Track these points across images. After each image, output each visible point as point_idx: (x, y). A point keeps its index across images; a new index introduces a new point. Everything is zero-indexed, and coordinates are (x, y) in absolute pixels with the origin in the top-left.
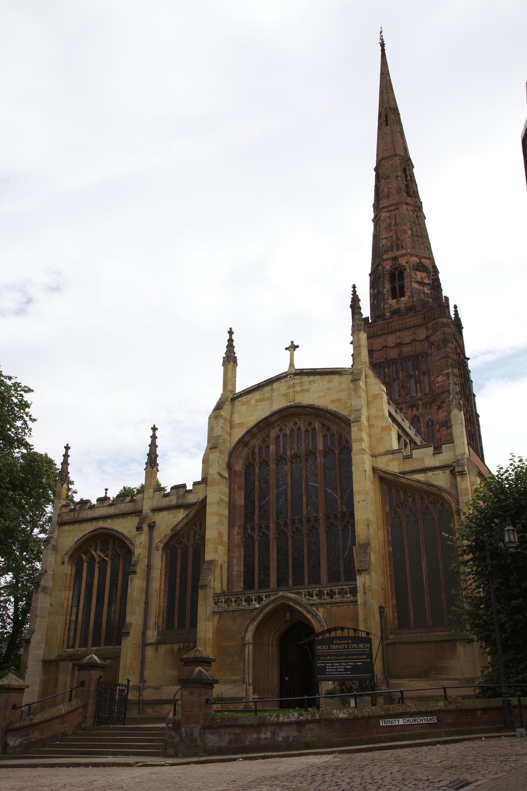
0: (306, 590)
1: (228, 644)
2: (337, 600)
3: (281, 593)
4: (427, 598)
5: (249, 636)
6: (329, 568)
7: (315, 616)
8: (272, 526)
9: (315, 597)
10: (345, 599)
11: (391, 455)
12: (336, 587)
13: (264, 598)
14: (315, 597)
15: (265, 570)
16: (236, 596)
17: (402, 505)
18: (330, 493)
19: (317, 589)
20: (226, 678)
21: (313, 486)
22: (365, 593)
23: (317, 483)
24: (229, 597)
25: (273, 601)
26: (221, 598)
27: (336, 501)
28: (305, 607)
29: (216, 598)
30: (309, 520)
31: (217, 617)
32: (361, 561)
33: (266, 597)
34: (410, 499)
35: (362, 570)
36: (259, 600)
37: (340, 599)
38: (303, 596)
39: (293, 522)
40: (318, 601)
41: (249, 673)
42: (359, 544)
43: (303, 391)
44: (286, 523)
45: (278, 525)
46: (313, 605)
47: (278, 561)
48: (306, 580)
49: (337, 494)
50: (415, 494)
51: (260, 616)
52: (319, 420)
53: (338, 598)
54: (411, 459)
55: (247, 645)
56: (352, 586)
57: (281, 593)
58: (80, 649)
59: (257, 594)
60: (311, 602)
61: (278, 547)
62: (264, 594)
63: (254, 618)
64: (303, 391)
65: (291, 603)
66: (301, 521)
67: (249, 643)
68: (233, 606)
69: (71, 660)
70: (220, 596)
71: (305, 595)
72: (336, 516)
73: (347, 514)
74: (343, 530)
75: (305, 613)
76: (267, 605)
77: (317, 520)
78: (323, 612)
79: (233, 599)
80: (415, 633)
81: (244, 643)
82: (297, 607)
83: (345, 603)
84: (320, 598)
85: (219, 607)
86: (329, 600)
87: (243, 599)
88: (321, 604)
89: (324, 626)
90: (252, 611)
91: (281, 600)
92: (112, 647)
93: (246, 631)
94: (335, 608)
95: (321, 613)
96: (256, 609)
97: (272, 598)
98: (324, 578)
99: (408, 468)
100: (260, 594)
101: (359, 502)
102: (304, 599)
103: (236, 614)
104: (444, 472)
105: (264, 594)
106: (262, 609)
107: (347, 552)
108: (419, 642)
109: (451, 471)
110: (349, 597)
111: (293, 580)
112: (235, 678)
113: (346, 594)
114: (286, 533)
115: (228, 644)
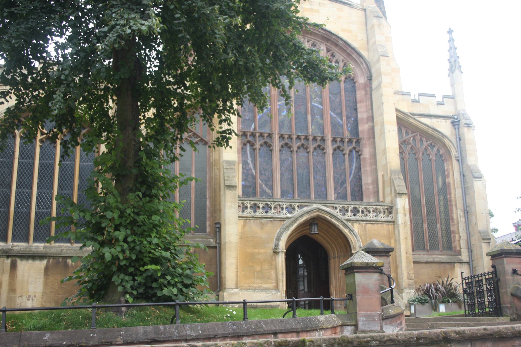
0: (341, 206)
1: (256, 251)
2: (372, 218)
3: (315, 206)
4: (425, 226)
5: (282, 245)
6: (335, 189)
7: (351, 230)
8: (276, 137)
9: (349, 213)
10: (379, 218)
11: (400, 96)
12: (371, 207)
13: (296, 209)
14: (349, 213)
15: (269, 181)
16: (264, 203)
17: (405, 142)
18: (335, 118)
19: (352, 206)
20: (255, 285)
21: (316, 106)
22: (405, 214)
23: (321, 104)
24: (256, 202)
25: (308, 212)
26: (245, 202)
27: (342, 126)
28: (342, 221)
29: (240, 202)
30: (315, 139)
31: (242, 222)
32: (399, 186)
33: (298, 206)
34: (412, 138)
35: (402, 194)
36: (291, 209)
37: (375, 218)
38: (338, 210)
39: (298, 138)
40: (353, 218)
41: (282, 281)
42: (391, 170)
43: (312, 10)
44: (290, 137)
45: (282, 137)
46: (348, 220)
47: (281, 174)
48: (313, 196)
49: (342, 120)
50: (416, 135)
51: (293, 225)
52: (326, 44)
53: (371, 216)
54: (418, 103)
55: (280, 254)
56: (386, 207)
57: (315, 206)
58: (15, 244)
59: (289, 204)
60: (346, 217)
61: (280, 160)
62: (297, 204)
63: (288, 227)
64: (312, 10)
65: (326, 217)
66: (306, 138)
67: (282, 252)
68: (260, 213)
69: (8, 257)
70: (245, 200)
71: (340, 210)
72: (342, 141)
73: (354, 140)
74: (349, 155)
75: (341, 227)
76: (302, 216)
77: (323, 140)
78: (359, 228)
79: (261, 206)
80: (419, 255)
81: (278, 251)
82: (334, 221)
83: (379, 221)
84: (355, 215)
85: (243, 211)
86: (364, 218)
87: (273, 207)
88: (357, 221)
89: (359, 241)
90: (283, 219)
91: (316, 212)
92: (69, 245)
93: (278, 239)
94: (369, 226)
95: (356, 227)
96: (288, 218)
97: (305, 209)
98: (332, 196)
99: (415, 111)
100: (293, 204)
101: (389, 131)
102: (339, 215)
103: (264, 221)
104: (446, 122)
105: (297, 204)
106: (296, 219)
107: (352, 176)
108: (427, 262)
109: (452, 123)
110: (381, 217)
111: (298, 194)
112: (266, 286)
113: (380, 212)
114: (290, 147)
115: (256, 251)
